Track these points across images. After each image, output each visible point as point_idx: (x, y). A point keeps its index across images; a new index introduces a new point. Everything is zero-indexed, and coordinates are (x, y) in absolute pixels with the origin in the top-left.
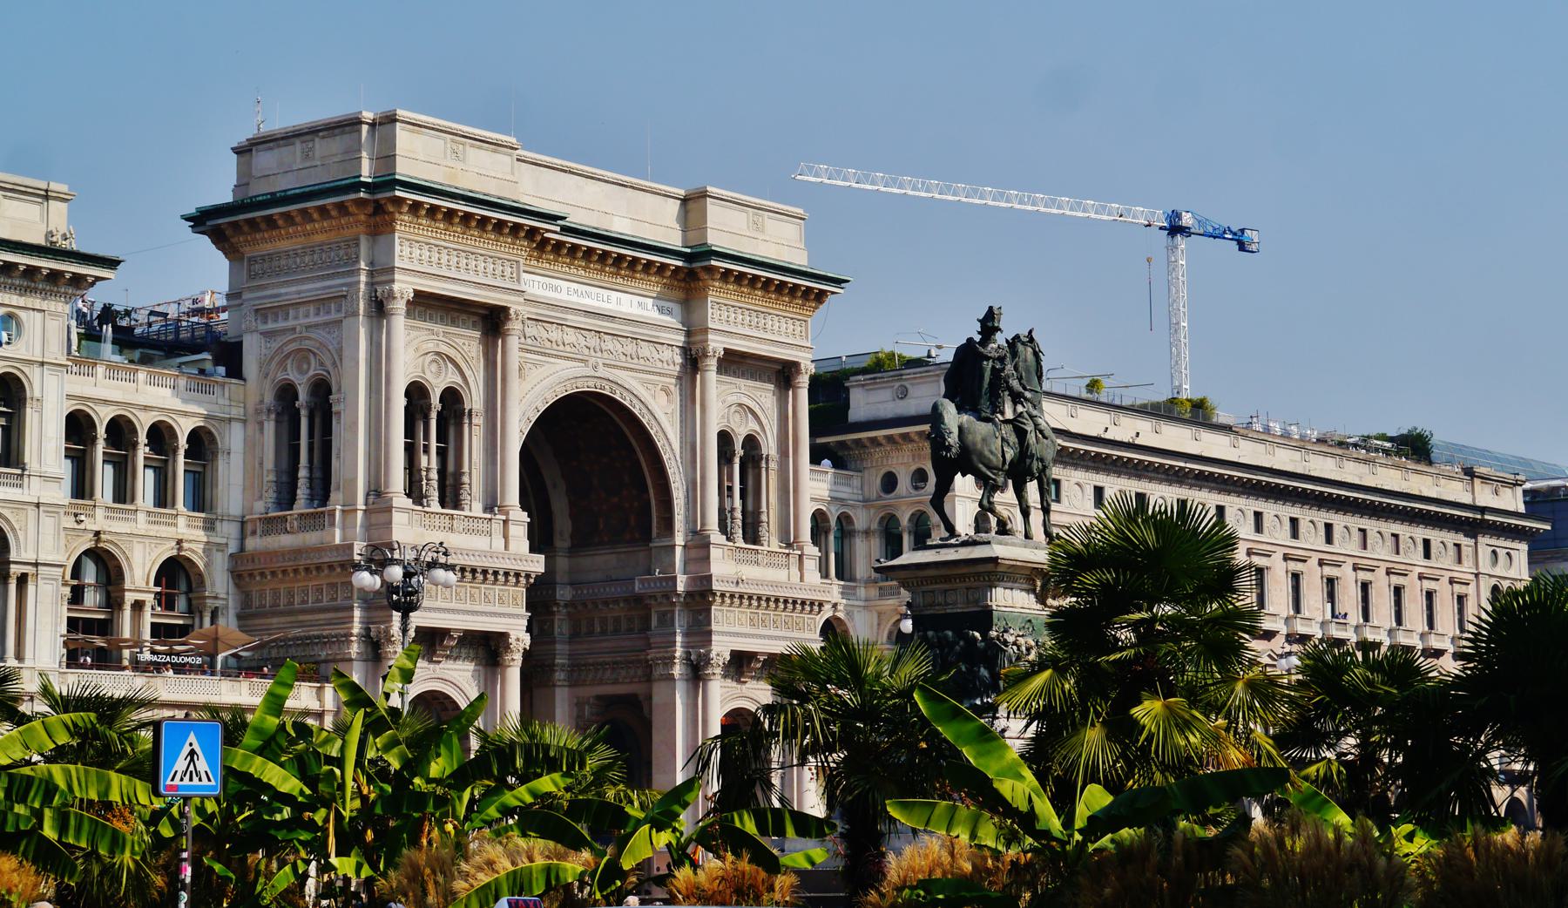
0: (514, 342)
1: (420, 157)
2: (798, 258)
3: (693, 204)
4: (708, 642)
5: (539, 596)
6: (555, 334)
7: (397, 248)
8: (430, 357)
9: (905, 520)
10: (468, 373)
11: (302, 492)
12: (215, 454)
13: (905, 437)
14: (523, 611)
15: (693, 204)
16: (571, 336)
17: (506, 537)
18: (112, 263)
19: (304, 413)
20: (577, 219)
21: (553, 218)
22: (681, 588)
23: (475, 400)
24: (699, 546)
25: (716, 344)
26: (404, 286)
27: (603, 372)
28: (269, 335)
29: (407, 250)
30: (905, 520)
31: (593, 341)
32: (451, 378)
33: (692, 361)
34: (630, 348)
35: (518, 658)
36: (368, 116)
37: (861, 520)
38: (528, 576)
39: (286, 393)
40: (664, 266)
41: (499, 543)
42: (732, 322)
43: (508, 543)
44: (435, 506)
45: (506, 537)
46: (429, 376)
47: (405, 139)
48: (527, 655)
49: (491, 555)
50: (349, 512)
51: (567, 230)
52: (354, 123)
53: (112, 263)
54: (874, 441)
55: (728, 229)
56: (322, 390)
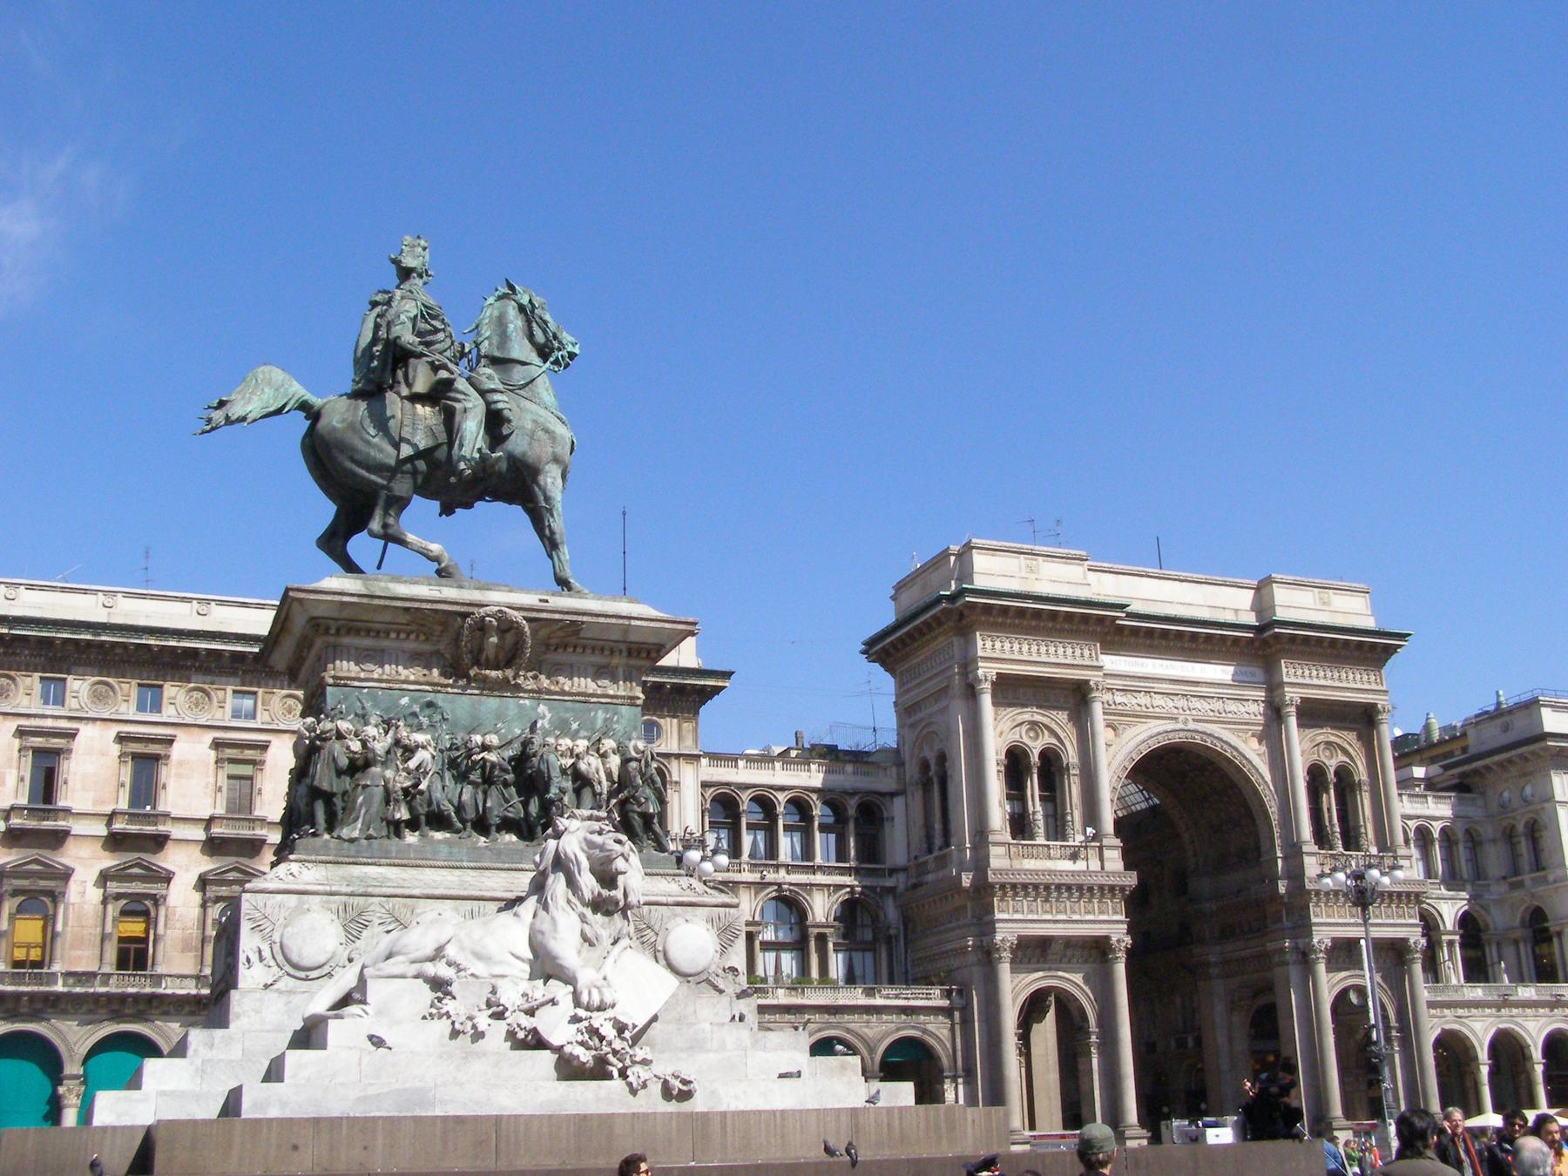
0: (1097, 709)
1: (994, 572)
2: (1369, 623)
3: (1262, 589)
4: (1310, 935)
5: (1137, 903)
6: (1143, 699)
7: (980, 643)
8: (1025, 728)
9: (1520, 828)
10: (1062, 735)
11: (938, 841)
12: (882, 820)
13: (1510, 761)
14: (1122, 918)
15: (1262, 589)
16: (1159, 700)
17: (1102, 859)
18: (727, 675)
19: (935, 780)
20: (1135, 607)
21: (1122, 607)
22: (1282, 890)
23: (1071, 756)
24: (1295, 853)
25: (1292, 695)
26: (986, 672)
27: (1192, 726)
28: (913, 726)
29: (989, 644)
30: (1520, 828)
31: (1182, 703)
32: (1046, 740)
33: (1275, 712)
34: (1217, 705)
35: (1122, 955)
36: (955, 548)
37: (1487, 831)
38: (1122, 889)
39: (925, 766)
40: (1236, 640)
41: (1095, 865)
42: (1304, 680)
43: (1111, 863)
44: (1041, 840)
45: (1102, 859)
46: (1026, 740)
47: (980, 561)
48: (1131, 954)
49: (1087, 873)
50: (962, 850)
51: (1131, 616)
52: (945, 554)
53: (727, 675)
54: (1488, 768)
55: (1297, 604)
56: (942, 758)
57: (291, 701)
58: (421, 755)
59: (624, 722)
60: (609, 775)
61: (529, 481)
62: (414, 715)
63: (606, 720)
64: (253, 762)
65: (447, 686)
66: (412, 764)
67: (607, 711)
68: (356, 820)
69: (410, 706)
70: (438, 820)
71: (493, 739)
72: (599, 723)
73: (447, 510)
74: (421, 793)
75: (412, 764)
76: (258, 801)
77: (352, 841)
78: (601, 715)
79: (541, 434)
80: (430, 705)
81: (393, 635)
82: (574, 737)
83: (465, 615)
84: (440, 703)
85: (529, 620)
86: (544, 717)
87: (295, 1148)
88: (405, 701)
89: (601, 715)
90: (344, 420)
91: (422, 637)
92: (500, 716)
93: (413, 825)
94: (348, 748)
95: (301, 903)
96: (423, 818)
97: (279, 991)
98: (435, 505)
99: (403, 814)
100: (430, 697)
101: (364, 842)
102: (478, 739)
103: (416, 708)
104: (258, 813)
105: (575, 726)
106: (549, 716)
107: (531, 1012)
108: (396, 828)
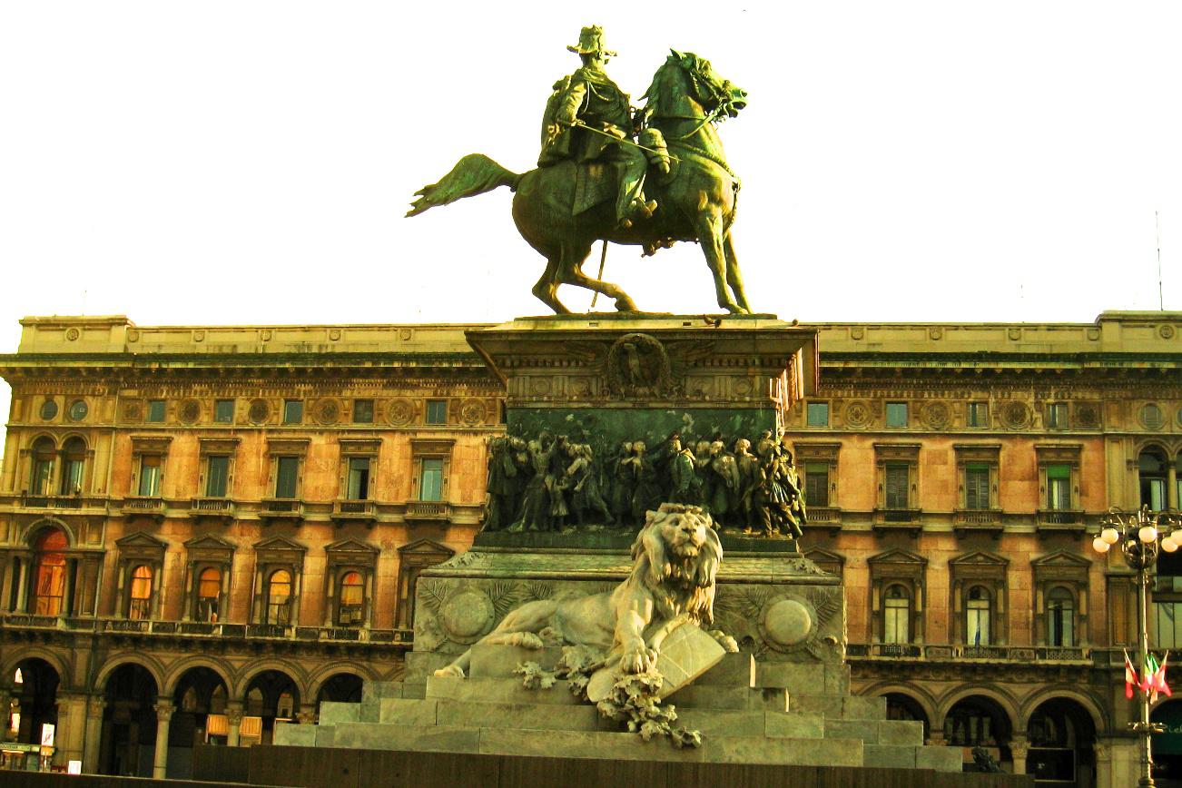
57: (857, 408)
60: (741, 470)
61: (692, 220)
62: (579, 429)
63: (743, 423)
64: (827, 462)
67: (744, 416)
68: (521, 518)
69: (574, 421)
70: (593, 515)
71: (640, 446)
72: (738, 426)
73: (648, 252)
75: (572, 469)
76: (832, 496)
77: (517, 533)
78: (739, 418)
79: (697, 178)
81: (557, 364)
82: (713, 439)
83: (611, 343)
85: (661, 341)
86: (688, 424)
87: (346, 771)
88: (570, 417)
89: (739, 418)
90: (529, 190)
92: (650, 426)
93: (571, 519)
95: (462, 584)
96: (580, 514)
97: (443, 654)
98: (639, 249)
102: (628, 446)
103: (580, 423)
104: (912, 506)
105: (715, 430)
106: (692, 422)
107: (588, 674)
108: (556, 524)
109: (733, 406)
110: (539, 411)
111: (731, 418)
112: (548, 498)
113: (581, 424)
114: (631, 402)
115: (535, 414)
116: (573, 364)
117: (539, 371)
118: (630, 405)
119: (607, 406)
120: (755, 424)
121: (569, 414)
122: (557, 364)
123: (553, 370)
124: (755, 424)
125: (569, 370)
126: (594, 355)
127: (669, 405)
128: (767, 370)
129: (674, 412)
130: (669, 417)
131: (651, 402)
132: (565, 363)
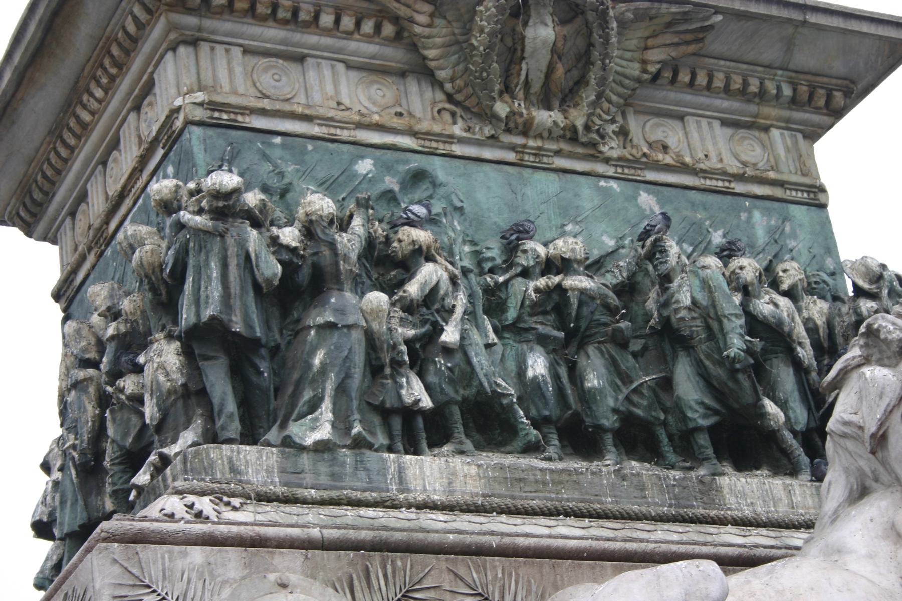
58: (429, 274)
59: (803, 235)
65: (450, 139)
66: (413, 289)
67: (767, 212)
68: (314, 405)
74: (447, 350)
77: (322, 447)
80: (418, 177)
84: (441, 176)
88: (365, 166)
91: (389, 29)
94: (274, 241)
99: (415, 391)
100: (417, 162)
101: (347, 456)
103: (391, 183)
109: (739, 188)
110: (278, 140)
111: (744, 216)
112: (379, 362)
113: (396, 188)
114: (513, 148)
115: (271, 145)
116: (368, 26)
117: (272, 33)
118: (511, 156)
119: (457, 149)
120: (794, 236)
121: (362, 157)
122: (327, 19)
123: (312, 39)
124: (794, 236)
125: (353, 45)
126: (428, 8)
127: (600, 168)
128: (798, 115)
129: (614, 185)
130: (606, 192)
131: (558, 153)
132: (348, 22)
